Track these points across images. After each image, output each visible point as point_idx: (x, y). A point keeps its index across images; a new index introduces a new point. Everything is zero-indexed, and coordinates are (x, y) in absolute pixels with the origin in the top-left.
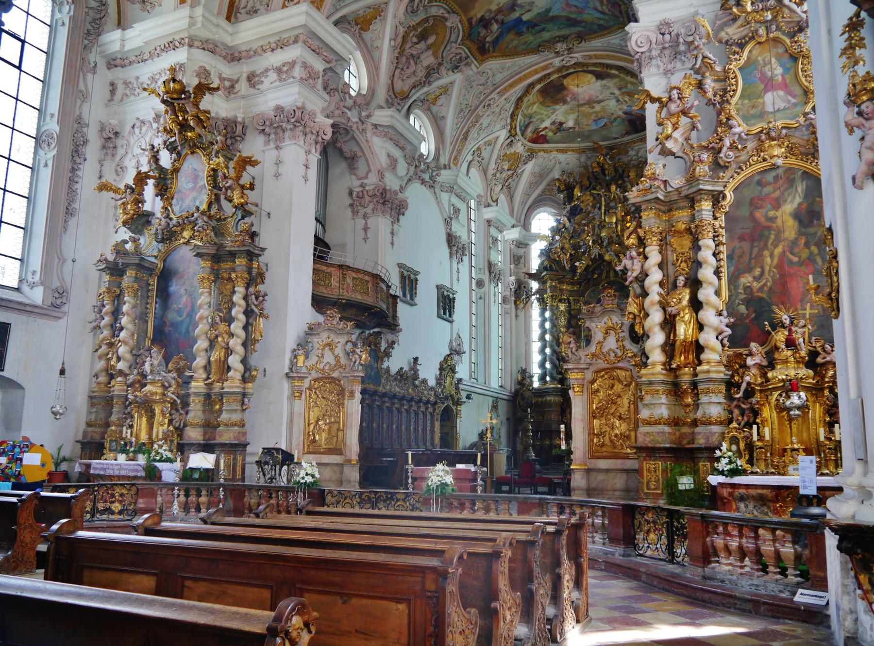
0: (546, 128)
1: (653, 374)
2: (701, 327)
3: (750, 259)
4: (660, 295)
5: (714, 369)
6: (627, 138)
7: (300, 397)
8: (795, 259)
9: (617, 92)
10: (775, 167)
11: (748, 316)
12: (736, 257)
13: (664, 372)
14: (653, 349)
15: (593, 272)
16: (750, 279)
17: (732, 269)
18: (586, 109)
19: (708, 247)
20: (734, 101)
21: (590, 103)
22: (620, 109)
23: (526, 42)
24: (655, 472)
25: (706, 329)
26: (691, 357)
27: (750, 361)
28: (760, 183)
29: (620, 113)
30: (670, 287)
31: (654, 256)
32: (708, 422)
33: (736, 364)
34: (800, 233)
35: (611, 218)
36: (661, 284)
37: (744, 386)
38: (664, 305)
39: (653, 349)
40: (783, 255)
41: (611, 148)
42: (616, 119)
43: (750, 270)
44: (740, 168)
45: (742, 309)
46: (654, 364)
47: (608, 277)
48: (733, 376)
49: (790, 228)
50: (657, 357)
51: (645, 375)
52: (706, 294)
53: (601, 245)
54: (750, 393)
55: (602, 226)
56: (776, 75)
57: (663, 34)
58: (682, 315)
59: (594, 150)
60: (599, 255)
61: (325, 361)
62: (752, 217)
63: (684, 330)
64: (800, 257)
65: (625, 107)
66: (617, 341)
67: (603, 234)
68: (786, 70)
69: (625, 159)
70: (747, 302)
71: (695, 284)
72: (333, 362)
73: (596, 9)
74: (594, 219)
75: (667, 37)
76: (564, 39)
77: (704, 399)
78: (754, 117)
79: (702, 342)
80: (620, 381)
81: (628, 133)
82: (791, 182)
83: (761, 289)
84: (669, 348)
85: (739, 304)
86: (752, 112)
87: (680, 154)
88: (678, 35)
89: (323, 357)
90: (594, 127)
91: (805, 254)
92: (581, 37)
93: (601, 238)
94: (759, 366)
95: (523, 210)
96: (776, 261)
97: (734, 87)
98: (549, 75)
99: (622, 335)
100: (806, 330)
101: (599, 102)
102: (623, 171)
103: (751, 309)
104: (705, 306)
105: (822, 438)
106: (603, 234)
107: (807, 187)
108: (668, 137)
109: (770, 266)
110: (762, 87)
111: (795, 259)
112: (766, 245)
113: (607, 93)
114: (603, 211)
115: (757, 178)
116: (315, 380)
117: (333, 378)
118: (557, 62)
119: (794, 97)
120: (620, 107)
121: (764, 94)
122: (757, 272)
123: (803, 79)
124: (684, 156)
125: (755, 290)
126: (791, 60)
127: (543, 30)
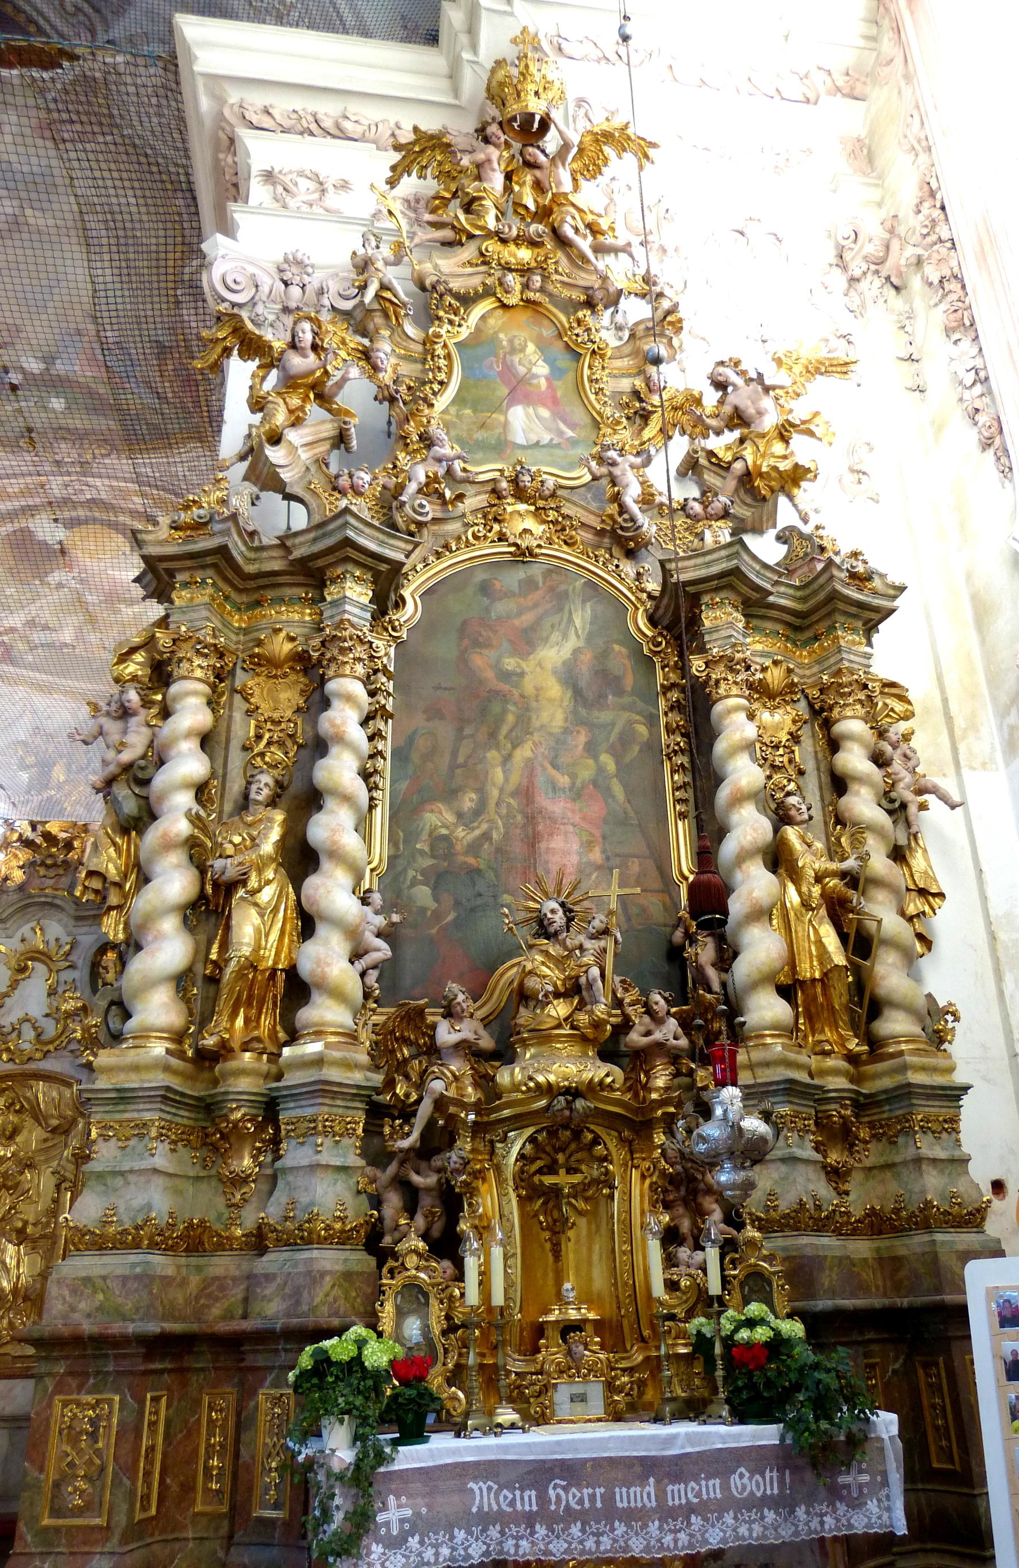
0: (12, 630)
1: (136, 1068)
2: (307, 924)
3: (453, 767)
4: (195, 820)
5: (337, 1054)
8: (564, 780)
10: (523, 555)
11: (437, 915)
12: (415, 757)
13: (174, 1062)
14: (150, 984)
16: (450, 818)
17: (404, 785)
19: (349, 698)
20: (442, 402)
24: (93, 1436)
25: (322, 930)
26: (266, 1022)
27: (446, 1034)
28: (485, 589)
30: (228, 807)
31: (192, 712)
32: (302, 1237)
33: (403, 1036)
34: (576, 720)
36: (201, 790)
37: (425, 1109)
38: (197, 853)
39: (150, 984)
40: (530, 767)
43: (450, 794)
44: (447, 547)
45: (423, 895)
46: (143, 1035)
48: (390, 1084)
49: (554, 709)
50: (158, 1009)
51: (109, 1070)
52: (333, 827)
54: (437, 1140)
56: (536, 376)
57: (286, 284)
58: (253, 883)
62: (463, 660)
63: (255, 930)
64: (573, 776)
66: (52, 993)
68: (556, 373)
70: (437, 880)
71: (306, 800)
73: (148, 384)
75: (295, 291)
76: (78, 437)
77: (295, 1154)
78: (481, 446)
79: (306, 968)
80: (37, 1116)
82: (560, 599)
83: (474, 848)
84: (201, 985)
85: (414, 883)
86: (480, 435)
87: (298, 490)
88: (321, 292)
91: (586, 772)
94: (466, 1049)
96: (515, 779)
97: (441, 376)
99: (68, 975)
100: (608, 943)
103: (447, 900)
104: (326, 864)
105: (658, 1290)
107: (594, 619)
108: (275, 439)
109: (502, 790)
110: (504, 391)
111: (564, 780)
112: (493, 735)
115: (480, 576)
119: (572, 426)
121: (509, 407)
122: (468, 801)
123: (592, 397)
124: (307, 497)
125: (458, 847)
126: (568, 356)
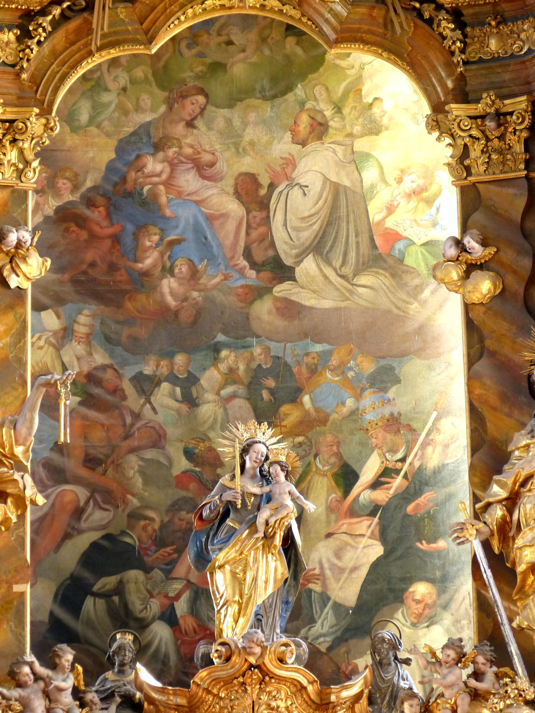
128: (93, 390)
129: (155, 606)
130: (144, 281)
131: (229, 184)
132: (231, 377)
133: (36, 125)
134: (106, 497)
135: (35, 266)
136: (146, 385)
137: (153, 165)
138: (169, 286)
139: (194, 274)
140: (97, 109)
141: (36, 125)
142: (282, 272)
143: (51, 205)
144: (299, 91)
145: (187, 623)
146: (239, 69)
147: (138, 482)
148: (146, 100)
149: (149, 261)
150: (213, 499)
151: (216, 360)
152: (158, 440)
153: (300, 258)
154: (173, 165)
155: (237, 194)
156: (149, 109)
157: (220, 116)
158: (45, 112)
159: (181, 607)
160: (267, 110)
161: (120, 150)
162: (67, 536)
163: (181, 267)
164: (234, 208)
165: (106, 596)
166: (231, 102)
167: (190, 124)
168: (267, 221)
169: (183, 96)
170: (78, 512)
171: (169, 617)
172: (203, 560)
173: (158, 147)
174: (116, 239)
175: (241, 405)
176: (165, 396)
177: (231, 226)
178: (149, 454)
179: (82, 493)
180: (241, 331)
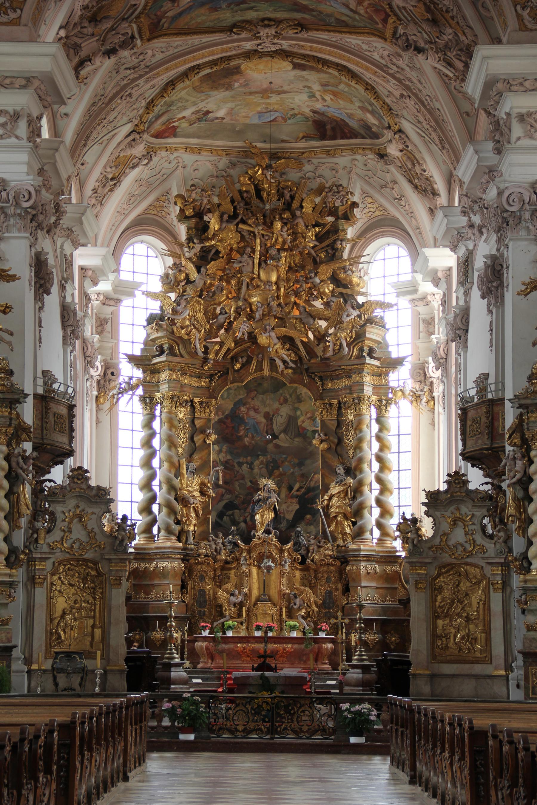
6: (303, 144)
7: (42, 584)
9: (316, 87)
15: (234, 359)
18: (257, 99)
21: (268, 91)
22: (308, 106)
23: (218, 19)
29: (307, 111)
35: (269, 274)
41: (274, 156)
42: (294, 116)
47: (260, 368)
53: (250, 317)
55: (253, 284)
59: (246, 153)
60: (250, 334)
61: (74, 536)
65: (318, 106)
67: (254, 299)
69: (293, 175)
72: (84, 538)
74: (240, 271)
81: (306, 137)
89: (70, 531)
90: (256, 121)
92: (302, 26)
93: (250, 305)
95: (111, 239)
98: (229, 58)
101: (279, 93)
102: (292, 197)
106: (254, 299)
113: (300, 85)
114: (256, 261)
116: (60, 563)
117: (86, 560)
118: (249, 45)
120: (310, 104)
127: (251, 8)
128: (227, 465)
129: (242, 519)
130: (240, 438)
131: (262, 414)
132: (262, 463)
133: (214, 402)
134: (229, 491)
135: (213, 437)
136: (240, 464)
137: (243, 409)
138: (246, 440)
139: (253, 437)
140: (229, 394)
141: (214, 402)
142: (275, 437)
143: (217, 418)
144: (281, 391)
145: (250, 523)
146: (265, 385)
147: (238, 488)
148: (241, 392)
149: (241, 433)
150: (256, 497)
151: (258, 458)
152: (243, 478)
153: (280, 433)
154: (248, 409)
155: (265, 417)
156: (242, 395)
157: (260, 397)
158: (216, 399)
159: (248, 519)
160: (272, 396)
161: (235, 404)
162: (220, 501)
163: (250, 435)
164: (263, 420)
165: (229, 516)
166: (263, 393)
167: (253, 399)
168: (272, 424)
169: (251, 391)
170: (223, 495)
171: (245, 521)
172: (253, 511)
173: (244, 404)
174: (233, 428)
175: (264, 470)
176: (245, 467)
177: (262, 425)
178: (241, 481)
179: (224, 491)
180: (265, 452)
